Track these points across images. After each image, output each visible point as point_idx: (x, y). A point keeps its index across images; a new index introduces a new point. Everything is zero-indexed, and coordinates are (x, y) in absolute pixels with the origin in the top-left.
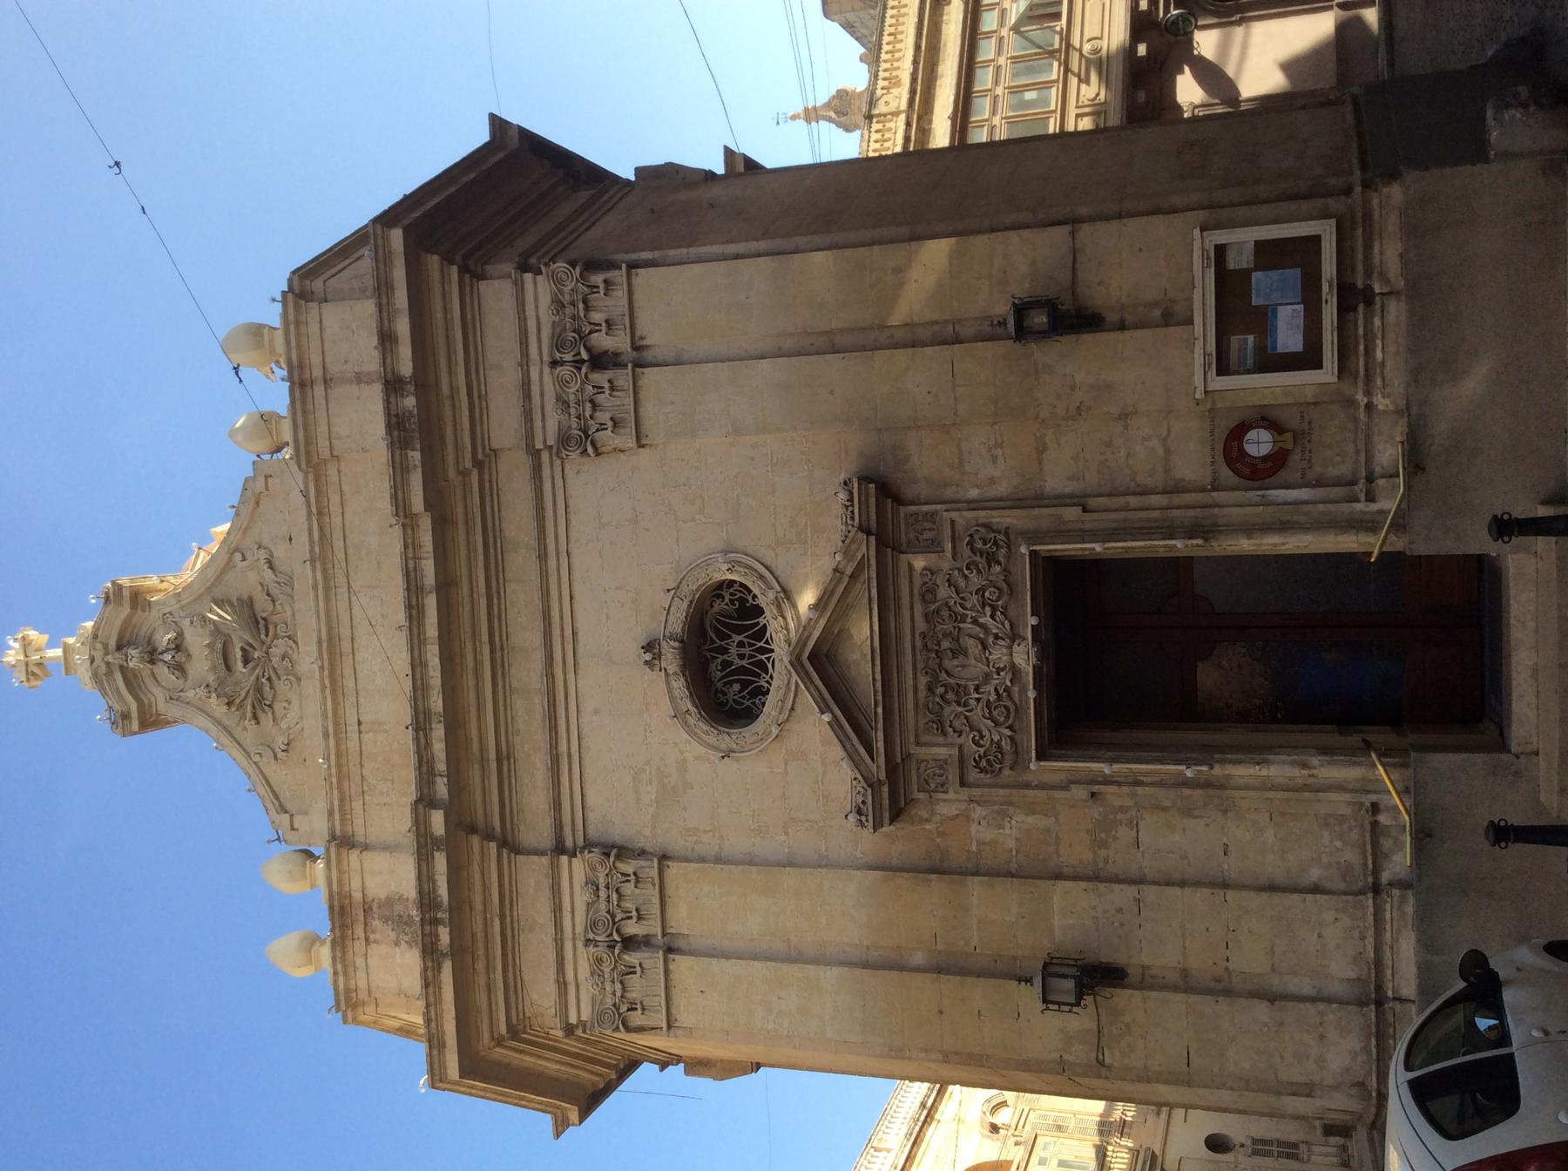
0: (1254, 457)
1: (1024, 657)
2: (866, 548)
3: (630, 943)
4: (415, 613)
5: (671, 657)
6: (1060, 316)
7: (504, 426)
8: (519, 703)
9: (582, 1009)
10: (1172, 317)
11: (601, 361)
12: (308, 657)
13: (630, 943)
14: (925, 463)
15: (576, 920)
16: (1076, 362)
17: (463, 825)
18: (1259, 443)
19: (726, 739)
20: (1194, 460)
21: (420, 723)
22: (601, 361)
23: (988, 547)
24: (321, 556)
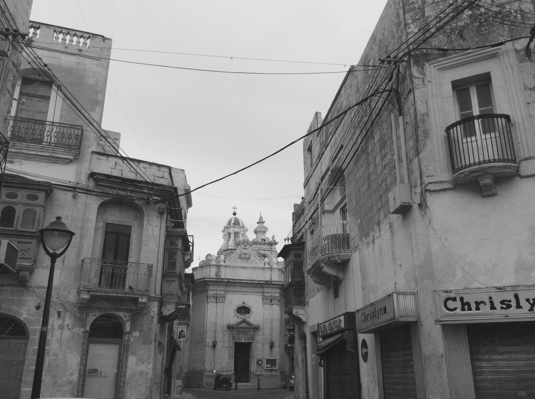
0: (259, 363)
1: (243, 341)
2: (254, 327)
3: (216, 298)
4: (251, 280)
5: (243, 305)
6: (272, 346)
7: (266, 290)
8: (239, 288)
9: (210, 292)
10: (271, 355)
11: (271, 301)
12: (245, 265)
13: (216, 298)
14: (260, 332)
15: (219, 293)
16: (267, 346)
17: (229, 282)
18: (260, 362)
19: (236, 310)
20: (259, 357)
21: (240, 280)
22: (271, 301)
23: (253, 338)
24: (255, 268)
